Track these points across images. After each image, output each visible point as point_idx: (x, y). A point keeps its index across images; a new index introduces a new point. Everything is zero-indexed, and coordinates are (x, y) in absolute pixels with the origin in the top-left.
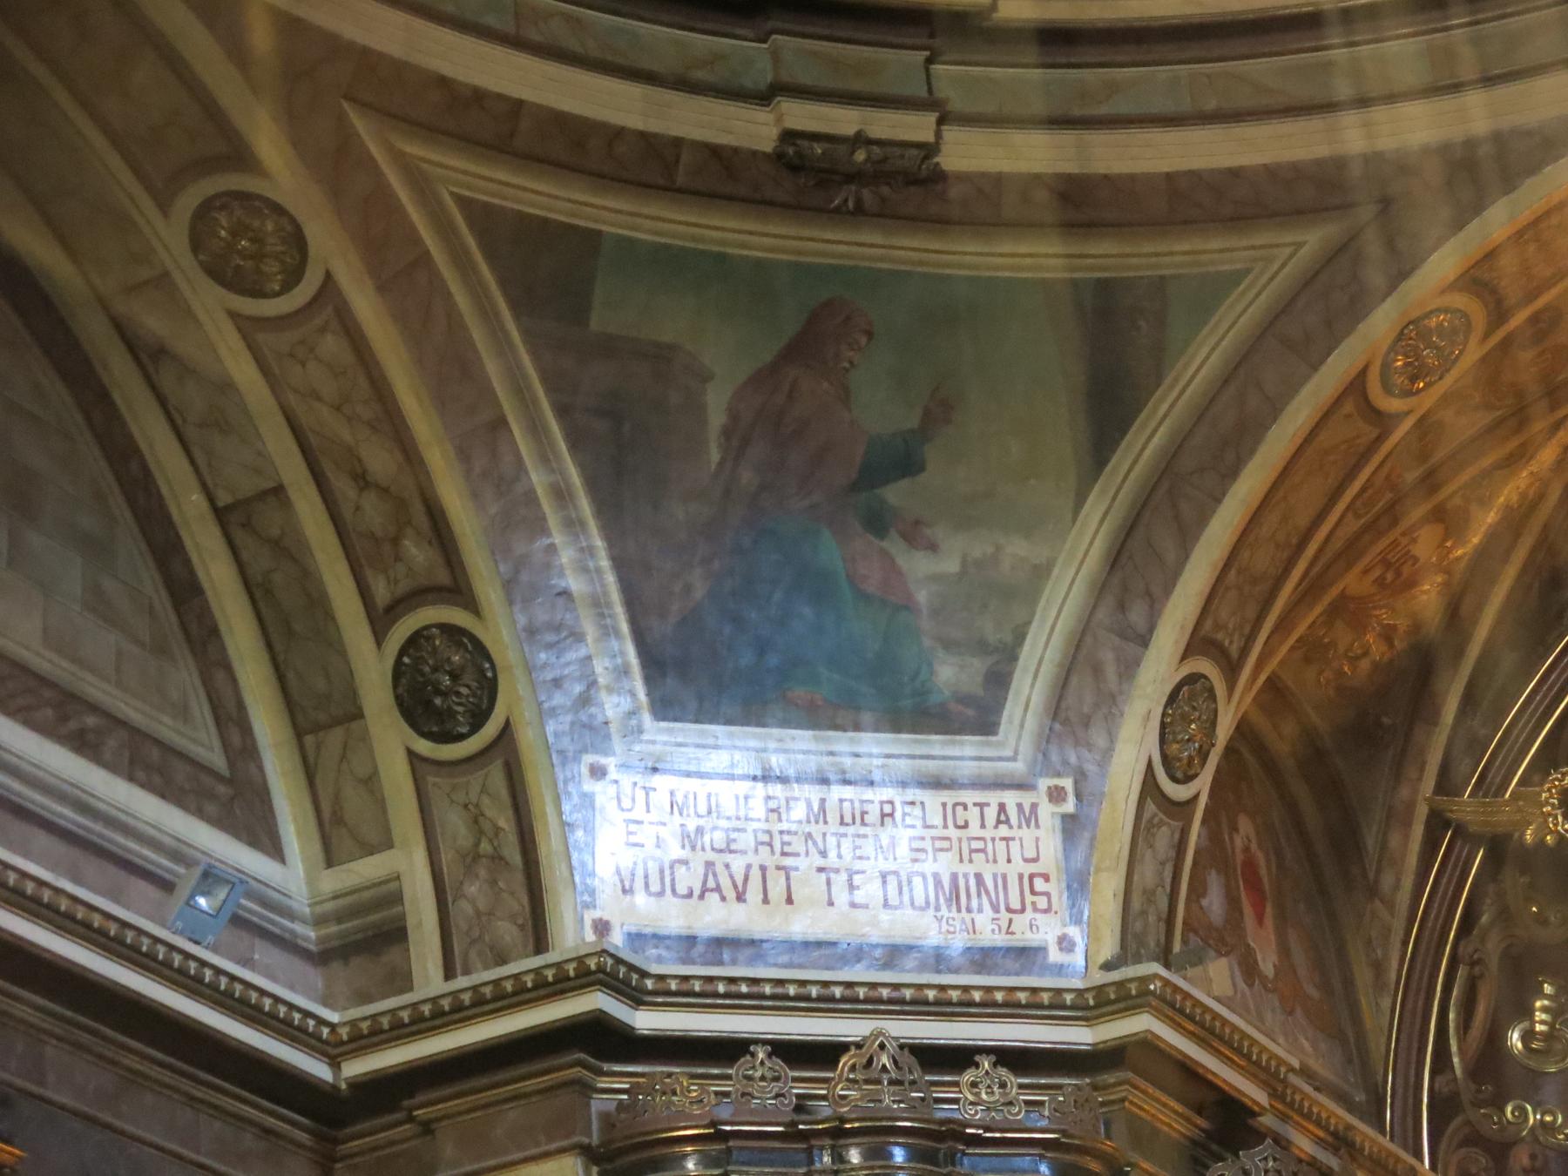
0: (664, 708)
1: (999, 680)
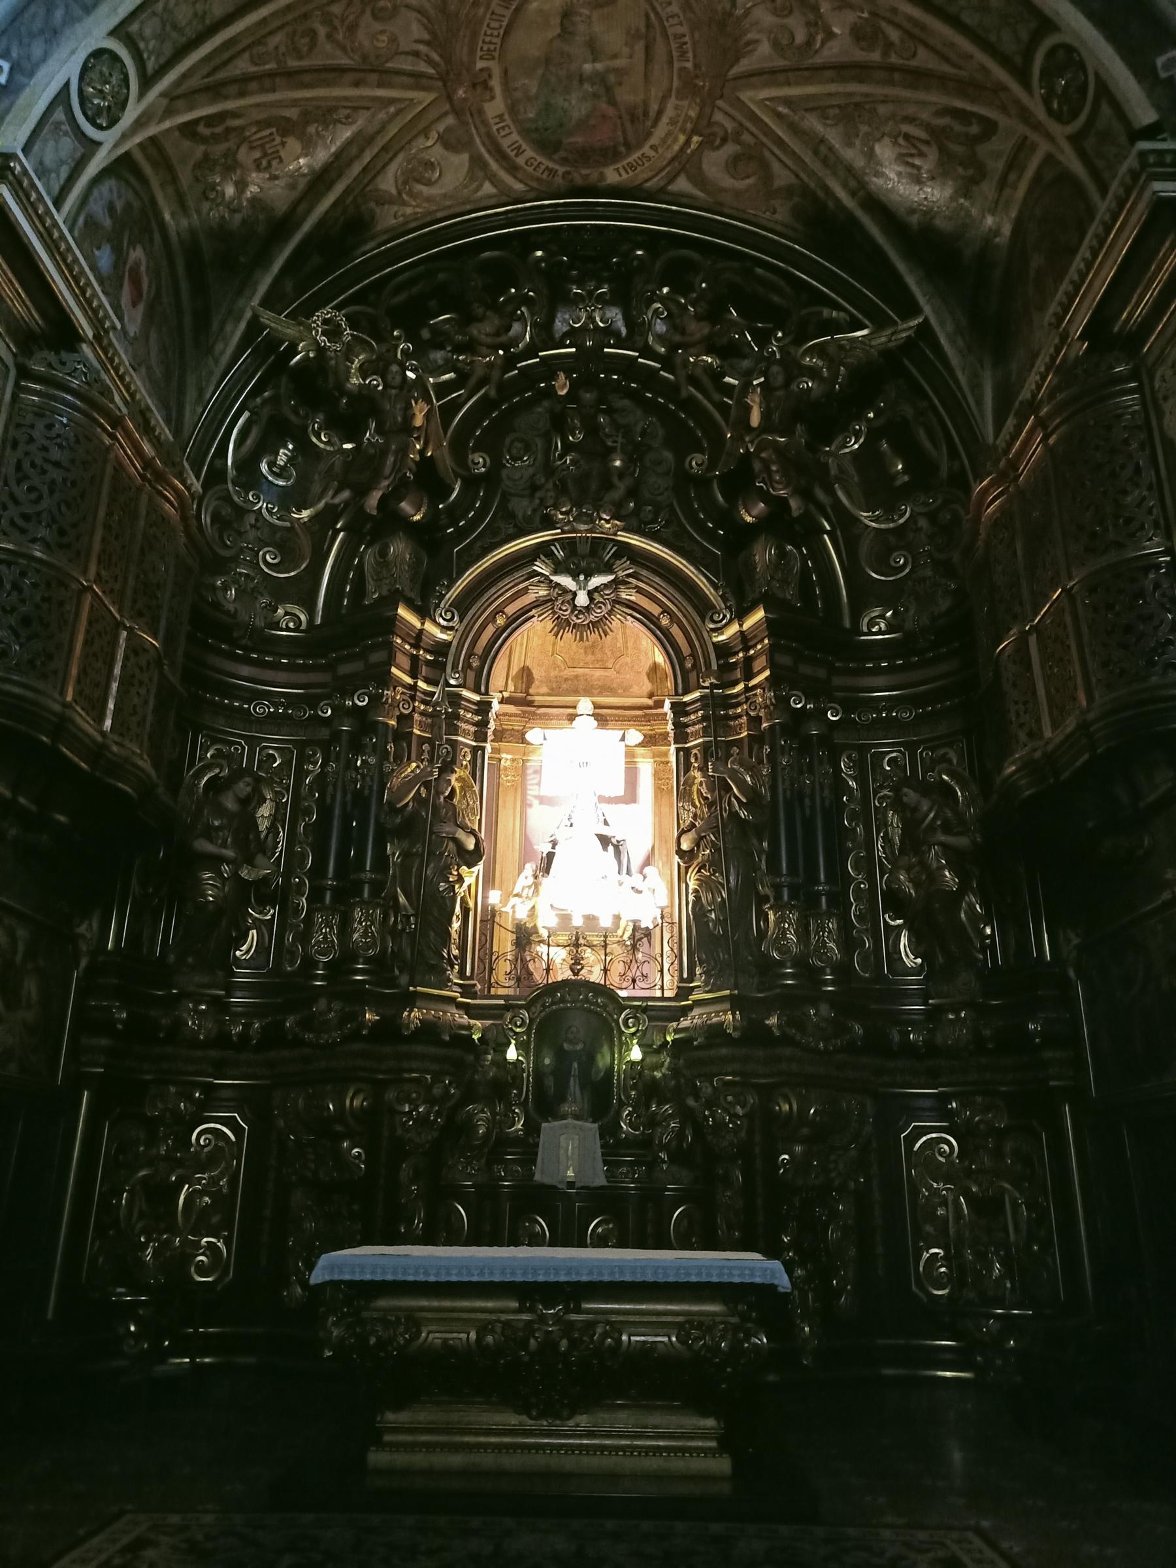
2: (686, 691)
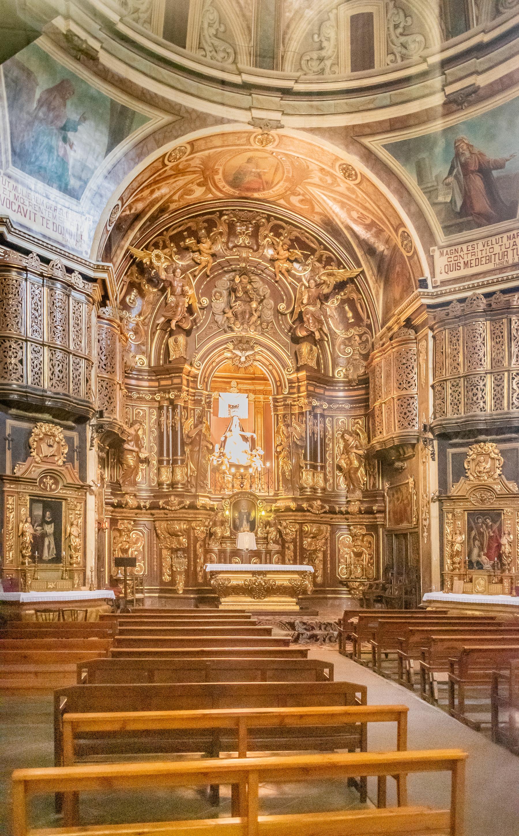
2: (278, 394)
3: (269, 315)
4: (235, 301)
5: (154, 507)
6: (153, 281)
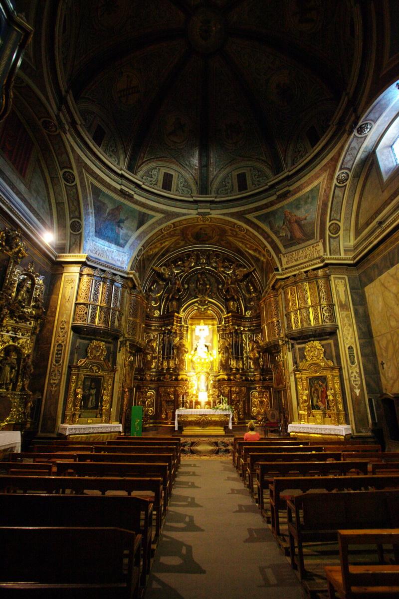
0: (96, 236)
1: (126, 243)
3: (215, 290)
4: (200, 285)
5: (159, 380)
6: (164, 280)
